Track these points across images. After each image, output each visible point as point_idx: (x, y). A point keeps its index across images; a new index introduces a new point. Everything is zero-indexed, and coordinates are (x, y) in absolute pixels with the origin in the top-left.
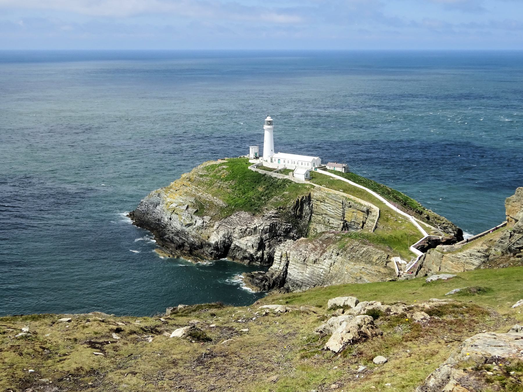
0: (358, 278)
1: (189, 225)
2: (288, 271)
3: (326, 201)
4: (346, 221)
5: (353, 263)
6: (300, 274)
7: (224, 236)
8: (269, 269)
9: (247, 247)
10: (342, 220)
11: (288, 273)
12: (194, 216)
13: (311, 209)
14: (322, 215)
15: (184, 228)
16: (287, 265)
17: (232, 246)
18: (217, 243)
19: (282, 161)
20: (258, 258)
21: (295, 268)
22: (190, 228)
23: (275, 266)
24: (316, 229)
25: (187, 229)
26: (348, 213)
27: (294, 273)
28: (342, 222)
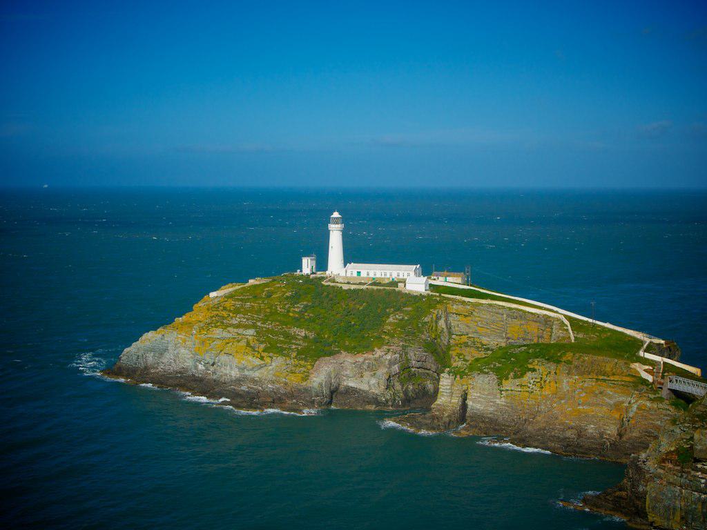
0: (597, 392)
1: (261, 367)
2: (469, 403)
3: (474, 313)
4: (508, 338)
5: (577, 377)
6: (492, 404)
7: (329, 375)
8: (433, 406)
9: (370, 386)
10: (503, 339)
11: (469, 407)
12: (264, 354)
13: (449, 328)
14: (467, 334)
15: (246, 373)
16: (465, 398)
17: (342, 388)
18: (321, 384)
19: (364, 274)
20: (387, 401)
21: (479, 397)
22: (263, 370)
23: (441, 400)
24: (461, 355)
25: (257, 374)
26: (513, 327)
27: (476, 405)
28: (505, 340)
